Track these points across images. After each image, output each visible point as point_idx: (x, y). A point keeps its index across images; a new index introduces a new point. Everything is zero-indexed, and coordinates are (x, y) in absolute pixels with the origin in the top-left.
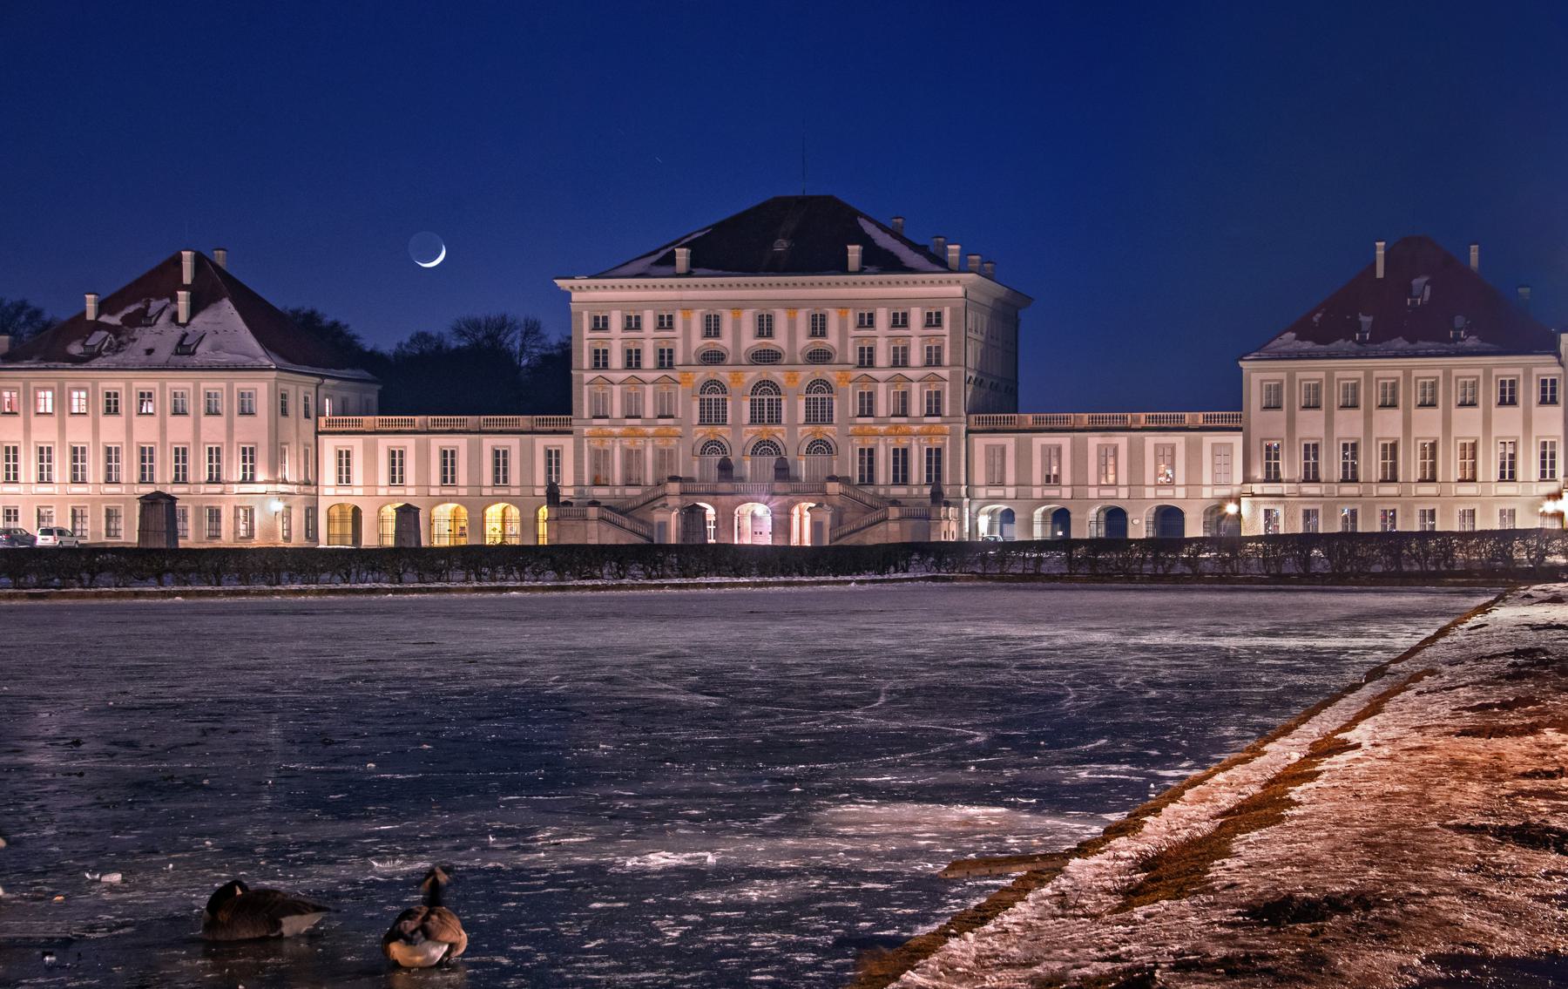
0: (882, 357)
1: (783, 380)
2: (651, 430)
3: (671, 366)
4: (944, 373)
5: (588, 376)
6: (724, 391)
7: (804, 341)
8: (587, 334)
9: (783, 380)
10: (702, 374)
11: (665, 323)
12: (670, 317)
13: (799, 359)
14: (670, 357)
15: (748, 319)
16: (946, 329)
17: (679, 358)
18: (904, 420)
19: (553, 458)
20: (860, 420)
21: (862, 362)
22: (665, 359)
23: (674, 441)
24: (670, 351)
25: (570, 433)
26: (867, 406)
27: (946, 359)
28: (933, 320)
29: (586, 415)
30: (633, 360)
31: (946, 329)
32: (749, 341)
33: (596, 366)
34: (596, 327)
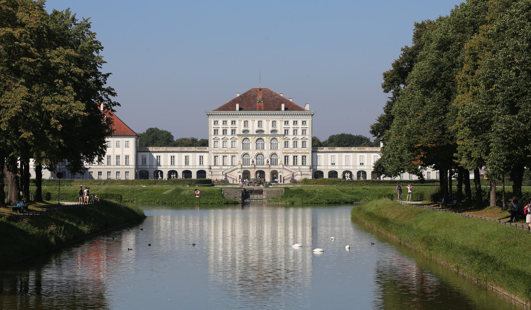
0: (291, 132)
2: (230, 152)
4: (307, 137)
7: (271, 128)
11: (233, 122)
12: (235, 121)
15: (256, 123)
17: (237, 132)
19: (201, 158)
25: (208, 152)
26: (286, 144)
28: (304, 123)
32: (256, 128)
34: (215, 124)
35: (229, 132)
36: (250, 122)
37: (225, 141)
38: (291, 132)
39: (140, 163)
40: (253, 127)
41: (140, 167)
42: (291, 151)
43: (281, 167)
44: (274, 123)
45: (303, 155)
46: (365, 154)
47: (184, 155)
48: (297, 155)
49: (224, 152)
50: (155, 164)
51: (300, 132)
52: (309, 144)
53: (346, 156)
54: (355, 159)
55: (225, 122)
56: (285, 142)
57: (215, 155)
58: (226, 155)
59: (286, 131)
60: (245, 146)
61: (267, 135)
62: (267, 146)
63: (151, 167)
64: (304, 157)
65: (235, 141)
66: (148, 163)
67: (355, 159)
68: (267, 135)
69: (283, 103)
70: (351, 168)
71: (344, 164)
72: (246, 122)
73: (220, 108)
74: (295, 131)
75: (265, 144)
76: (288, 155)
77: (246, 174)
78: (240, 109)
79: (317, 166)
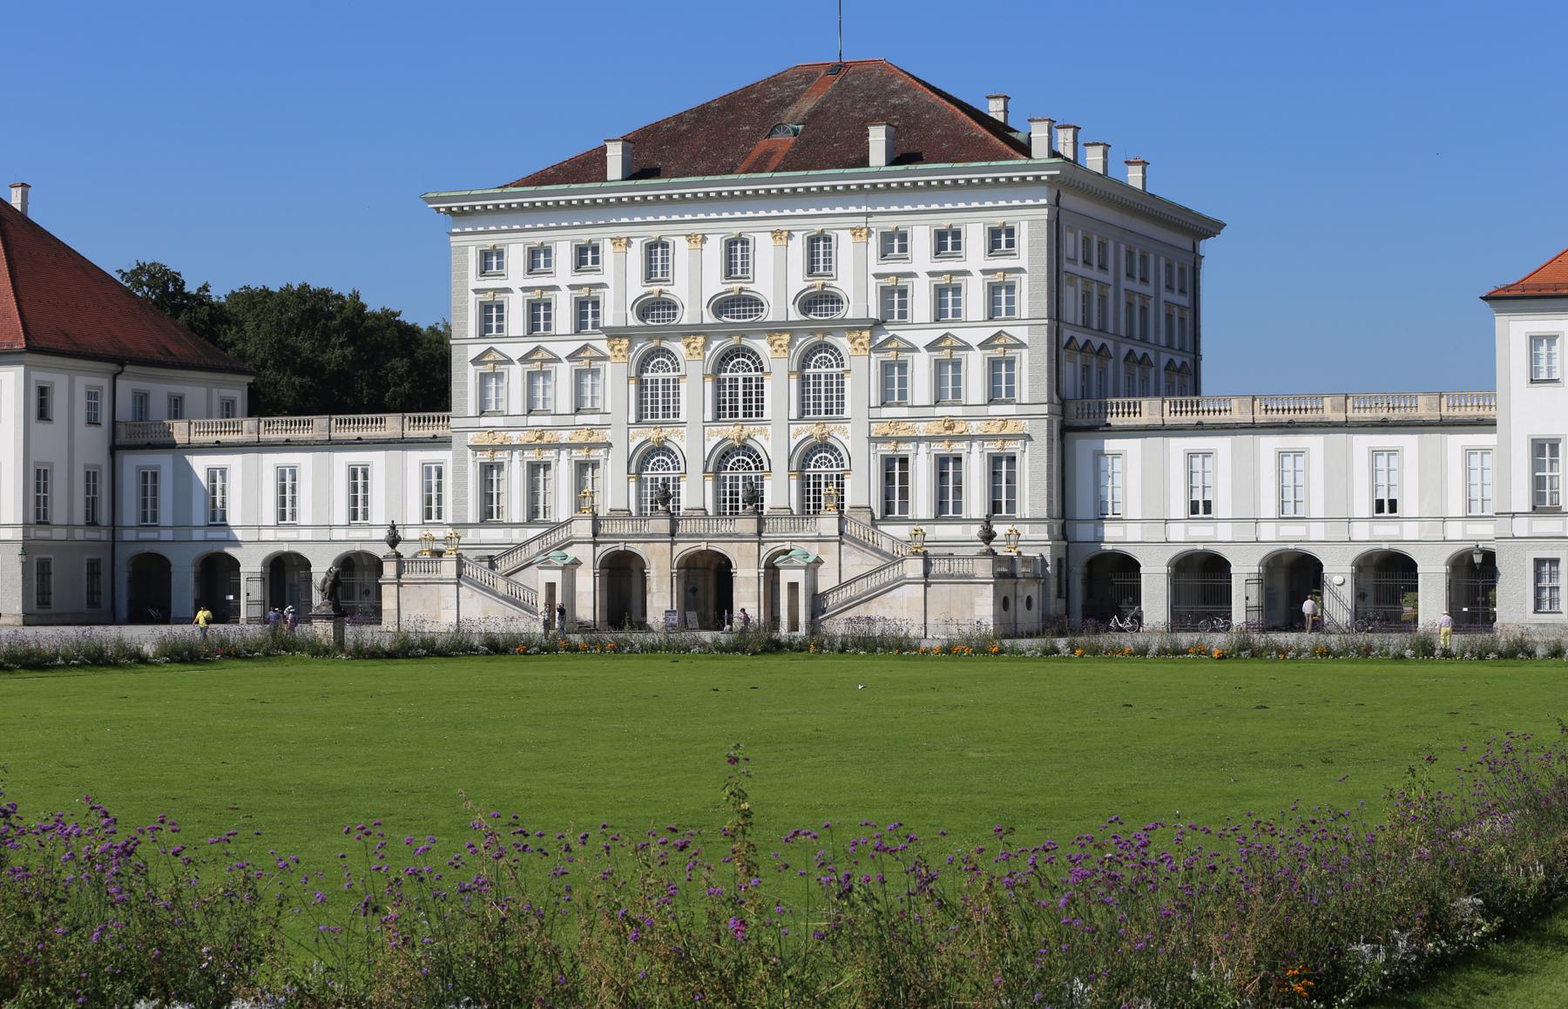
0: (921, 303)
2: (564, 436)
4: (1021, 333)
5: (474, 351)
7: (798, 282)
11: (585, 256)
14: (596, 315)
15: (714, 250)
17: (609, 318)
18: (957, 411)
20: (887, 412)
23: (601, 452)
27: (1024, 306)
28: (1000, 239)
32: (715, 285)
34: (484, 270)
35: (563, 317)
36: (681, 250)
37: (538, 369)
38: (921, 303)
40: (696, 279)
41: (129, 535)
42: (922, 429)
44: (818, 247)
45: (994, 447)
46: (1408, 443)
47: (342, 460)
49: (529, 437)
50: (199, 516)
52: (1031, 375)
53: (1282, 454)
54: (1339, 476)
55: (537, 258)
56: (886, 367)
57: (485, 457)
58: (549, 455)
59: (894, 295)
60: (653, 402)
61: (773, 330)
62: (779, 392)
63: (183, 535)
64: (1000, 467)
65: (595, 372)
66: (165, 517)
67: (1339, 476)
68: (773, 330)
69: (874, 120)
70: (1317, 531)
71: (1269, 508)
72: (656, 252)
73: (559, 168)
74: (946, 296)
76: (905, 449)
77: (622, 574)
78: (637, 171)
79: (1100, 518)
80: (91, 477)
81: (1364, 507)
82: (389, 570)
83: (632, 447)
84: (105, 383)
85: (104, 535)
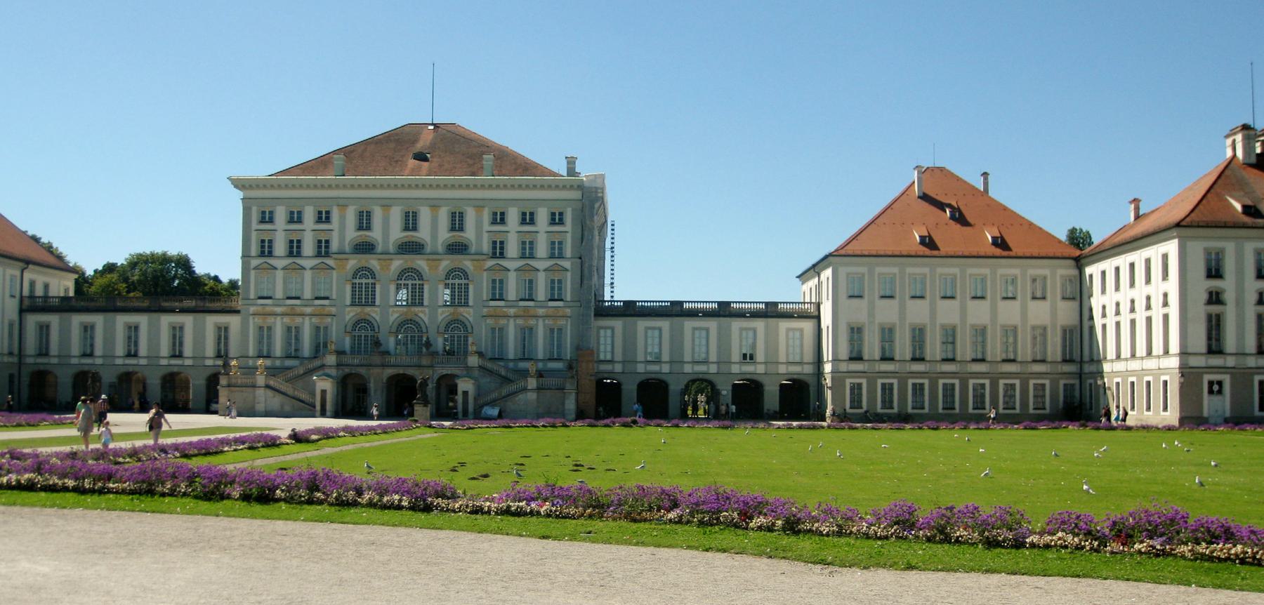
0: (512, 249)
1: (426, 269)
2: (308, 310)
3: (327, 255)
4: (567, 264)
6: (374, 277)
7: (444, 235)
8: (255, 225)
9: (426, 269)
10: (353, 263)
11: (323, 217)
12: (328, 213)
13: (440, 249)
14: (327, 247)
16: (568, 226)
17: (334, 246)
20: (492, 303)
21: (494, 253)
22: (323, 249)
23: (329, 320)
24: (327, 242)
25: (238, 312)
27: (568, 251)
29: (252, 296)
30: (294, 249)
31: (568, 226)
33: (262, 254)
35: (308, 248)
39: (31, 345)
41: (30, 360)
43: (473, 361)
47: (166, 320)
48: (532, 322)
51: (542, 249)
66: (54, 349)
75: (426, 287)
80: (11, 325)
81: (736, 357)
82: (223, 381)
83: (348, 318)
84: (18, 273)
85: (15, 360)
